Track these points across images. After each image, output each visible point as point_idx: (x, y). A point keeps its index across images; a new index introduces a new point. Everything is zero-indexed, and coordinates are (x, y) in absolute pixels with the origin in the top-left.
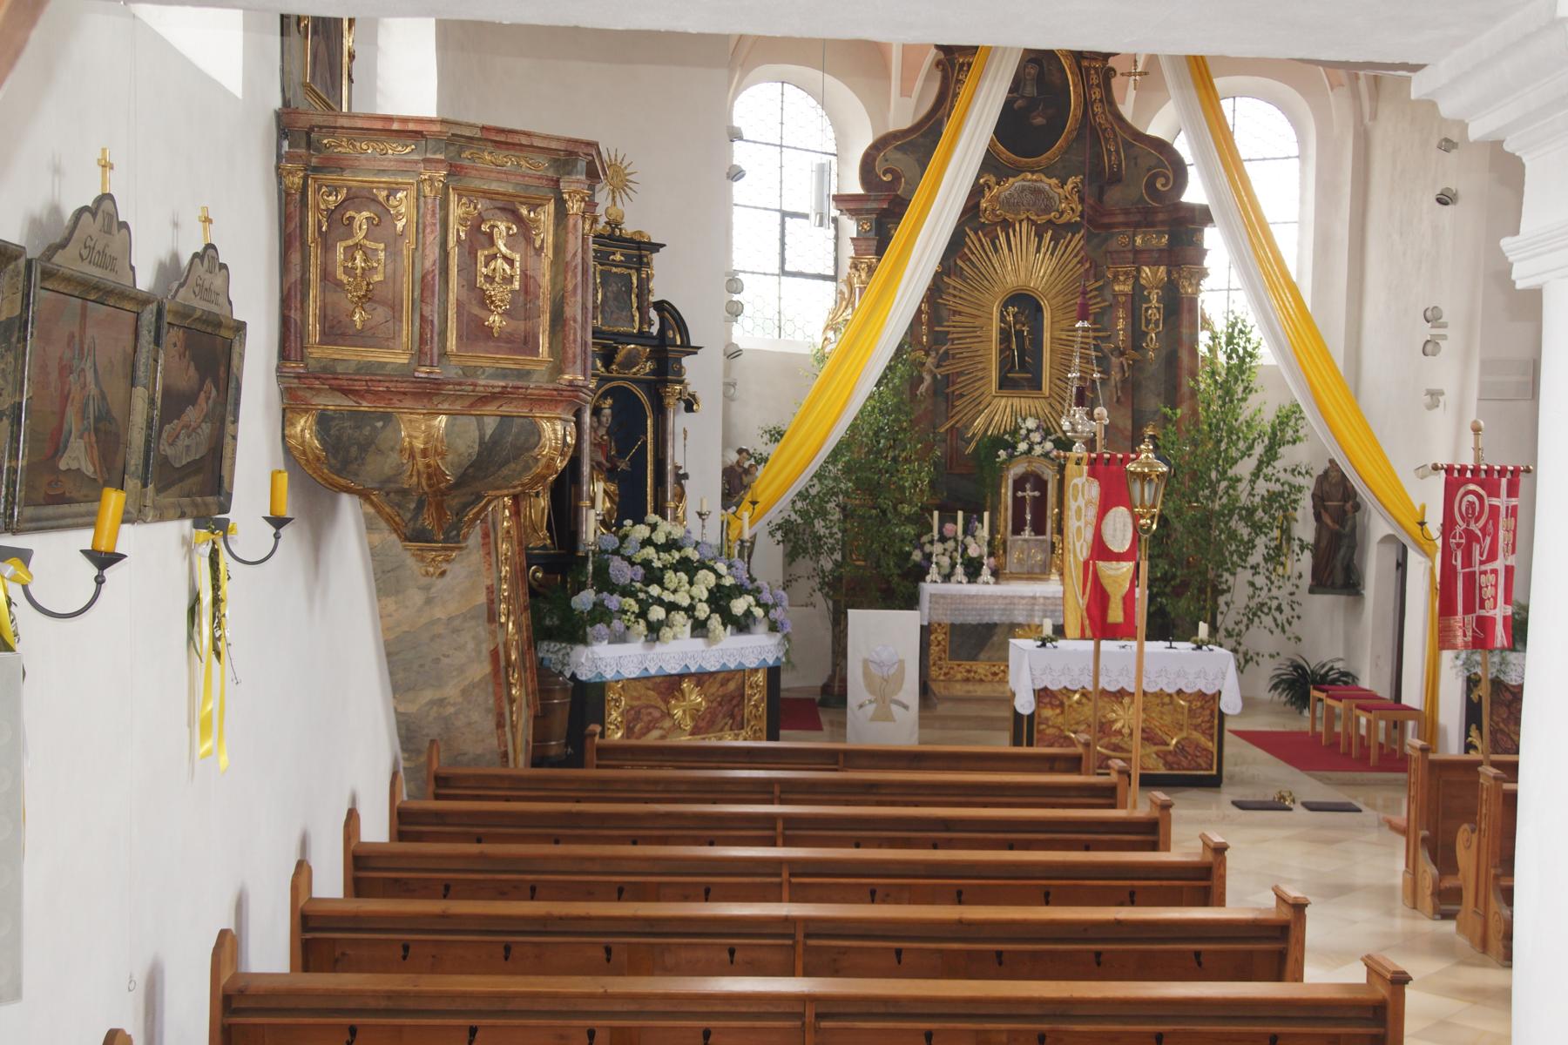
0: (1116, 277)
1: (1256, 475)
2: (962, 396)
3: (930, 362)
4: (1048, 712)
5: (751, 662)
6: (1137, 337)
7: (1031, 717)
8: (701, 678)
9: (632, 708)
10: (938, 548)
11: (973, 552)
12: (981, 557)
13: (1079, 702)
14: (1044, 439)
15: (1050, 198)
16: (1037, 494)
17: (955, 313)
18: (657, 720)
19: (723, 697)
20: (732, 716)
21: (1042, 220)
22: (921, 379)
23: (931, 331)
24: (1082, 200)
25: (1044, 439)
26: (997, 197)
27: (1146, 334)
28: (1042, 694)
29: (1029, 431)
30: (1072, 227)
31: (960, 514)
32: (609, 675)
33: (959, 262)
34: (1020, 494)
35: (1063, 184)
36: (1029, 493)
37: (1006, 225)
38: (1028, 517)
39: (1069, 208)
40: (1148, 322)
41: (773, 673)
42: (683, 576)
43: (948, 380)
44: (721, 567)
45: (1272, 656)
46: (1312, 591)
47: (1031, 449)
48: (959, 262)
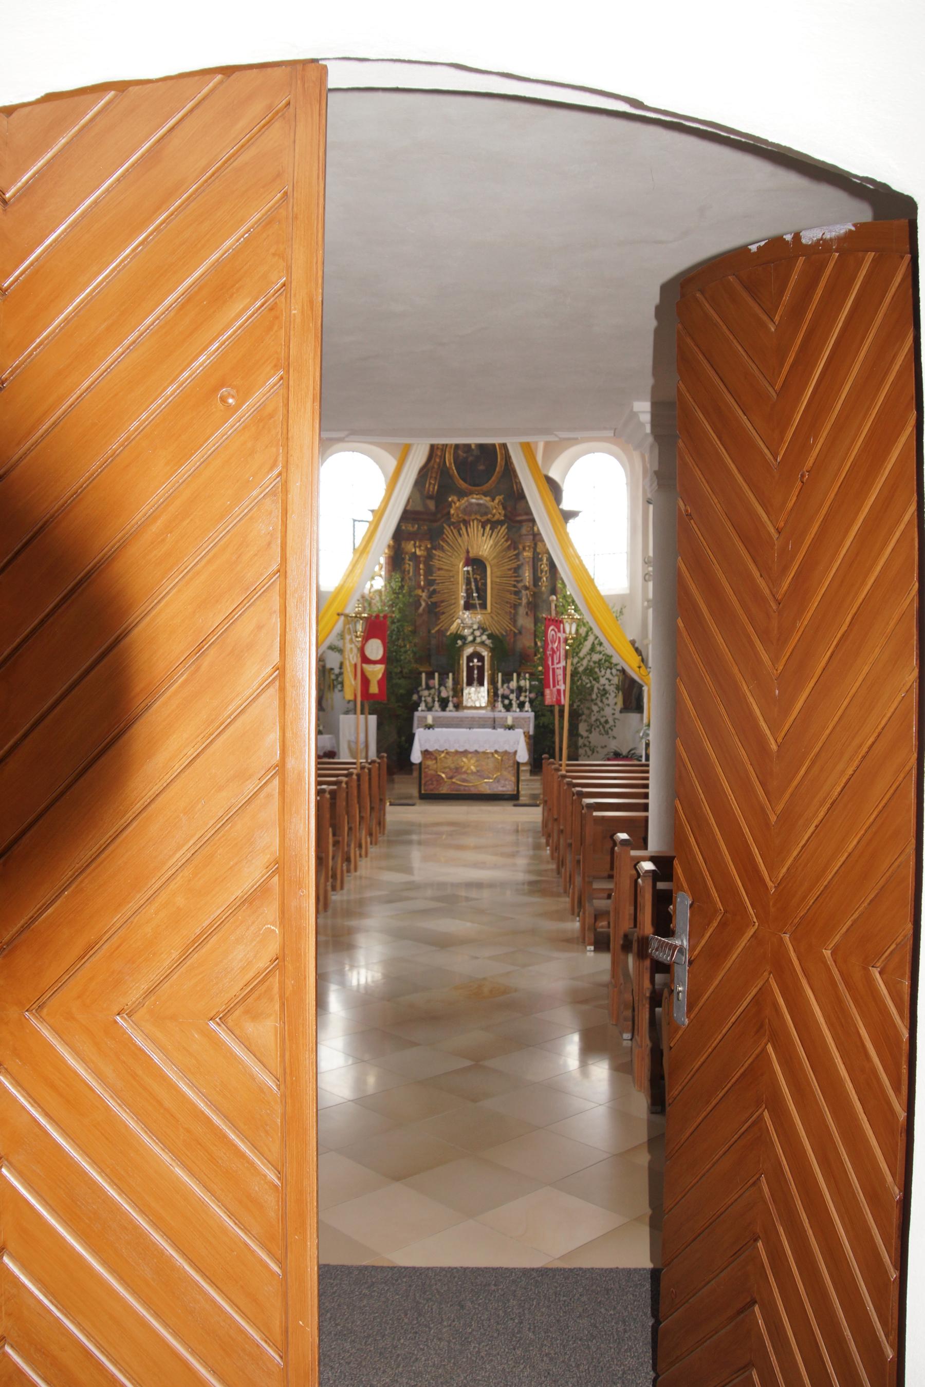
0: (524, 549)
1: (592, 649)
2: (443, 613)
3: (424, 595)
4: (430, 763)
6: (536, 579)
7: (420, 764)
10: (426, 693)
11: (444, 694)
12: (448, 697)
13: (445, 757)
14: (482, 634)
15: (487, 507)
16: (480, 664)
17: (440, 569)
21: (484, 519)
22: (420, 605)
23: (426, 579)
24: (504, 508)
25: (482, 634)
26: (457, 509)
27: (541, 578)
28: (426, 753)
30: (500, 523)
31: (436, 675)
33: (441, 543)
35: (493, 500)
37: (466, 523)
38: (475, 676)
39: (498, 513)
40: (542, 571)
43: (435, 605)
45: (602, 747)
46: (621, 712)
47: (474, 639)
48: (441, 543)
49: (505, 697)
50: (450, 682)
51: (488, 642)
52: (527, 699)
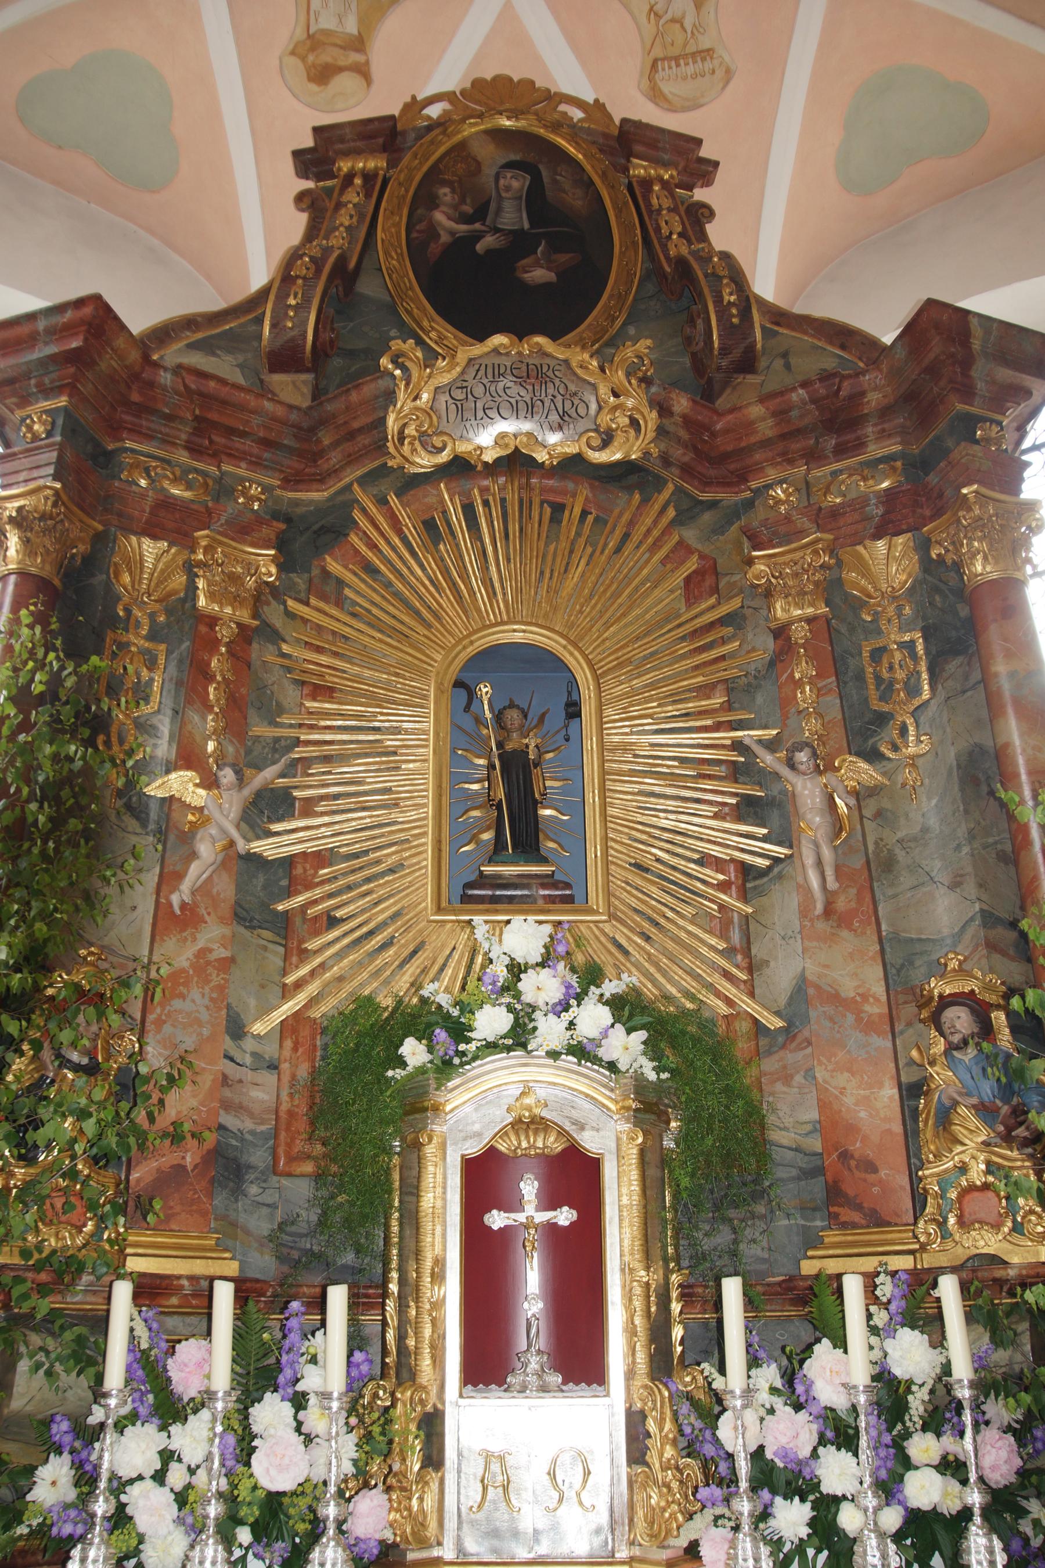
2: (333, 922)
10: (131, 1452)
11: (278, 1467)
16: (565, 1216)
29: (517, 970)
34: (496, 1220)
36: (529, 1210)
47: (520, 1036)
49: (780, 1479)
50: (327, 1363)
51: (626, 1047)
52: (975, 1498)
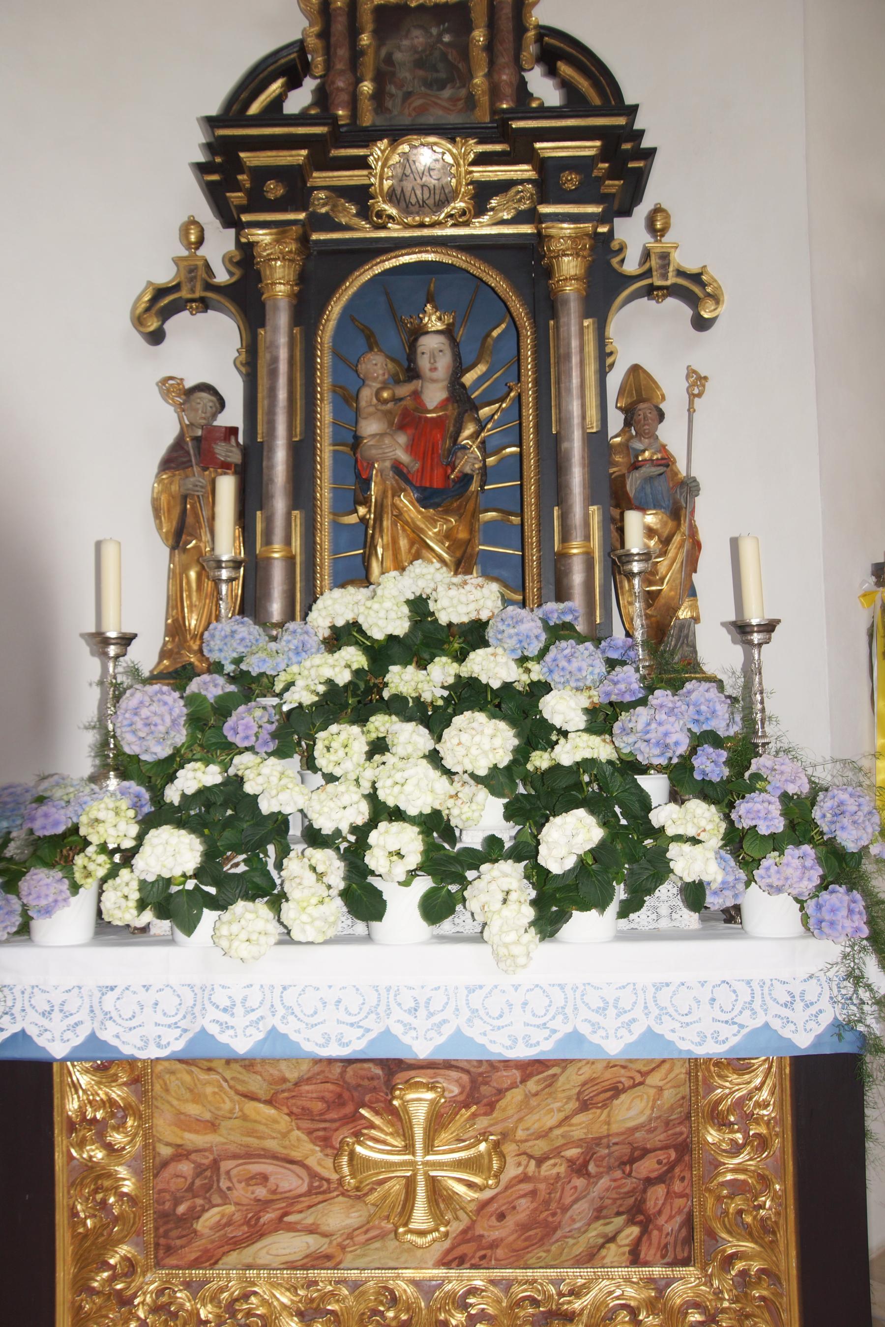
5: (703, 1036)
8: (480, 1085)
9: (182, 1153)
18: (292, 1201)
19: (591, 1146)
20: (638, 1213)
32: (56, 1046)
41: (823, 1087)
42: (410, 737)
44: (563, 708)
